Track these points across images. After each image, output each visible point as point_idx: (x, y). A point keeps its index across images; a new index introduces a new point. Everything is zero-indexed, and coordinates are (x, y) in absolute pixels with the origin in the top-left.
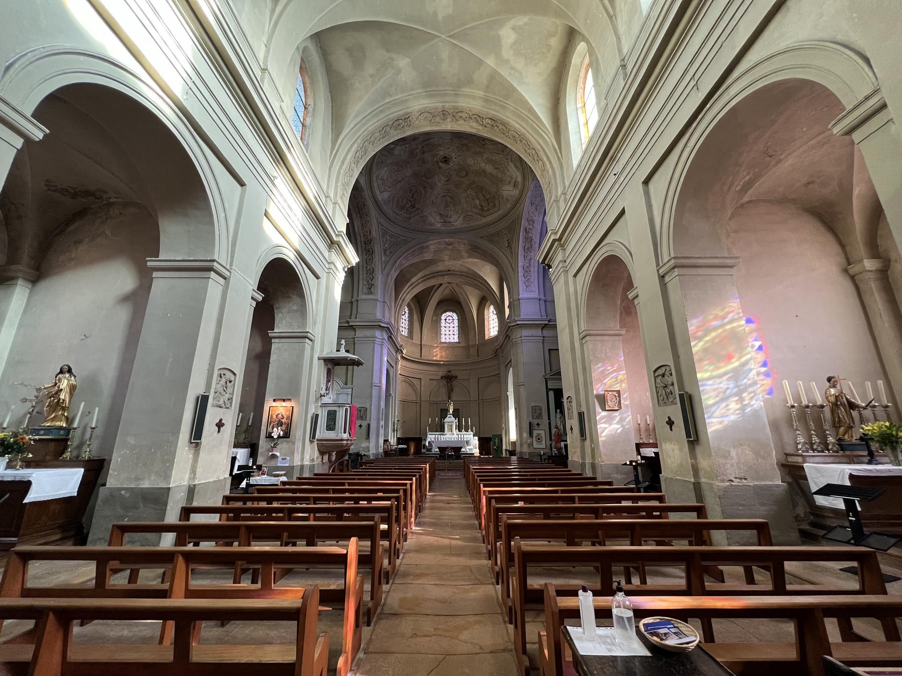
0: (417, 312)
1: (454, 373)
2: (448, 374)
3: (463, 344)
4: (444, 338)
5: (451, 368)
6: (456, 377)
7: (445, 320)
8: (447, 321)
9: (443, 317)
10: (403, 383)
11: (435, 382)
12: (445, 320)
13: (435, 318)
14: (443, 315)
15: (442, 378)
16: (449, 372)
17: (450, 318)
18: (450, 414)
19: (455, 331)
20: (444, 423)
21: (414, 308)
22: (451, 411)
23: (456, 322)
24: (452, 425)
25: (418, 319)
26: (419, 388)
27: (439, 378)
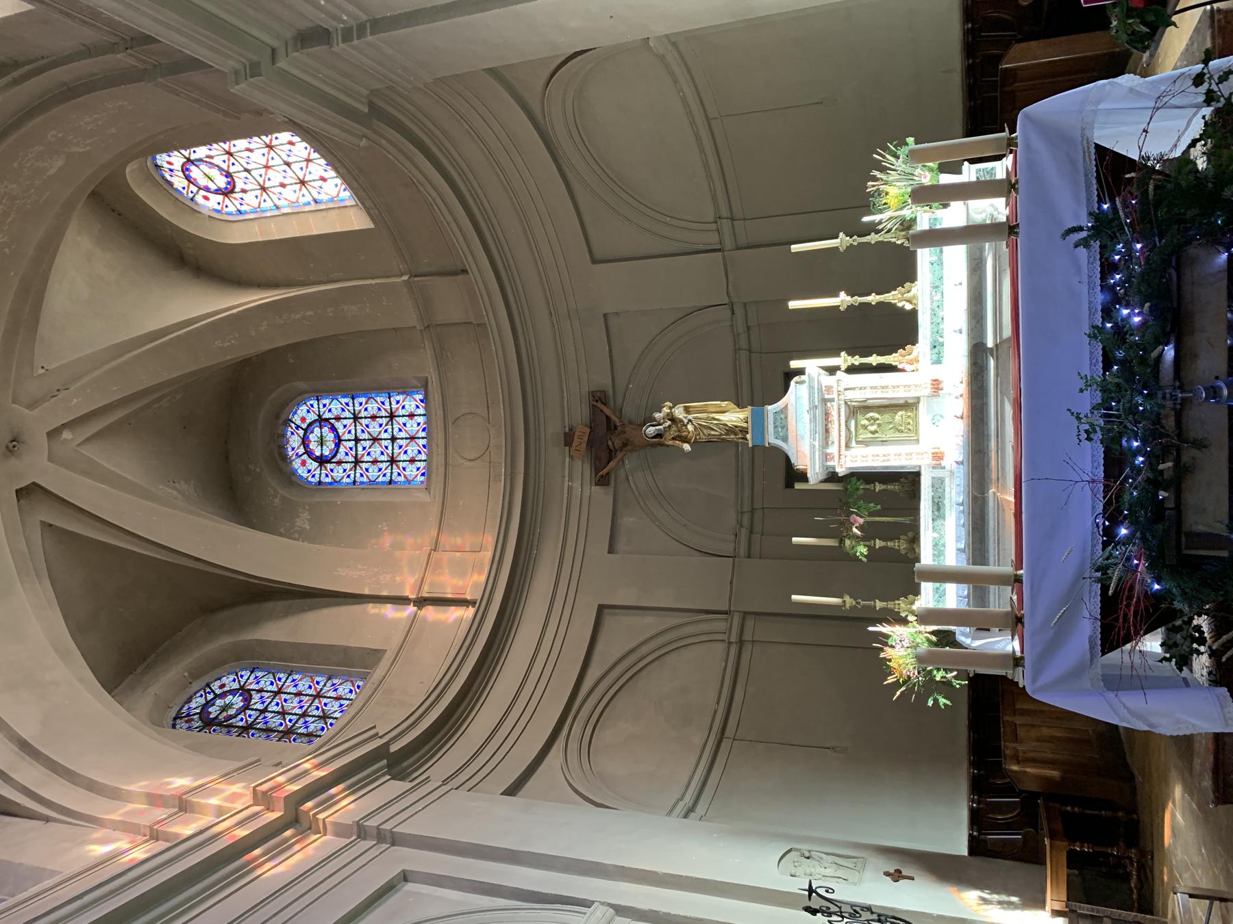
0: (256, 622)
1: (579, 414)
2: (581, 441)
3: (424, 362)
4: (411, 471)
5: (553, 428)
6: (598, 398)
7: (322, 461)
8: (326, 453)
9: (305, 469)
10: (606, 735)
11: (628, 521)
12: (322, 461)
13: (303, 521)
14: (302, 472)
15: (603, 481)
16: (568, 439)
17: (313, 437)
18: (759, 422)
19: (372, 407)
20: (832, 477)
21: (225, 640)
22: (734, 416)
23: (334, 406)
24: (857, 410)
25: (286, 614)
26: (650, 624)
27: (603, 496)
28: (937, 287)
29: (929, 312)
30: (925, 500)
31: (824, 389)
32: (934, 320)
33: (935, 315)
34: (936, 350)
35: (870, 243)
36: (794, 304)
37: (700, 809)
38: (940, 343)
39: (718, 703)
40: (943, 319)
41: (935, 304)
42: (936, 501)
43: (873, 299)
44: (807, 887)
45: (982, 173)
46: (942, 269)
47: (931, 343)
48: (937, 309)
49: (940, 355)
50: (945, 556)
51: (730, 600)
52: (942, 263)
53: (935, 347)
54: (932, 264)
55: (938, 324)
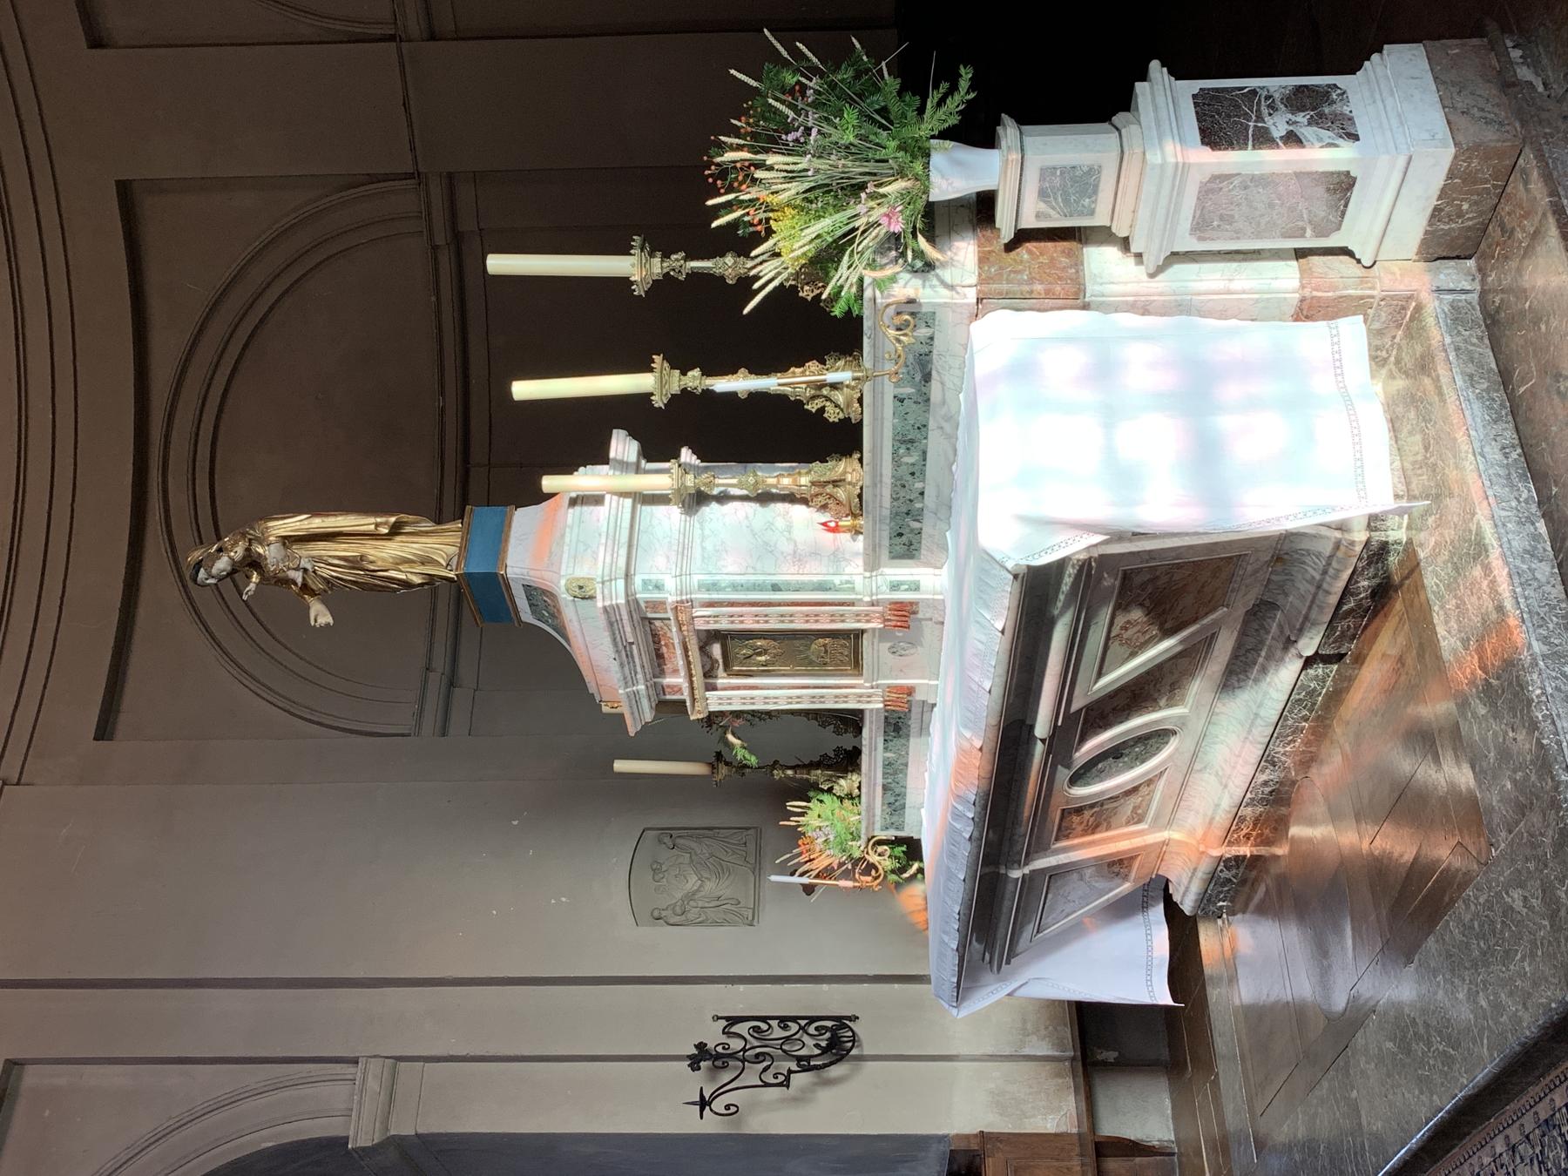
28: (912, 441)
29: (887, 479)
30: (871, 722)
31: (643, 605)
32: (902, 494)
33: (904, 486)
34: (904, 538)
35: (722, 278)
36: (524, 390)
37: (466, 671)
38: (912, 530)
39: (442, 393)
40: (922, 494)
41: (904, 470)
42: (893, 721)
43: (740, 383)
44: (697, 1099)
45: (1057, 182)
46: (926, 411)
47: (891, 529)
48: (909, 478)
49: (912, 547)
50: (906, 774)
51: (413, 149)
52: (928, 400)
53: (901, 535)
54: (902, 401)
55: (911, 501)
